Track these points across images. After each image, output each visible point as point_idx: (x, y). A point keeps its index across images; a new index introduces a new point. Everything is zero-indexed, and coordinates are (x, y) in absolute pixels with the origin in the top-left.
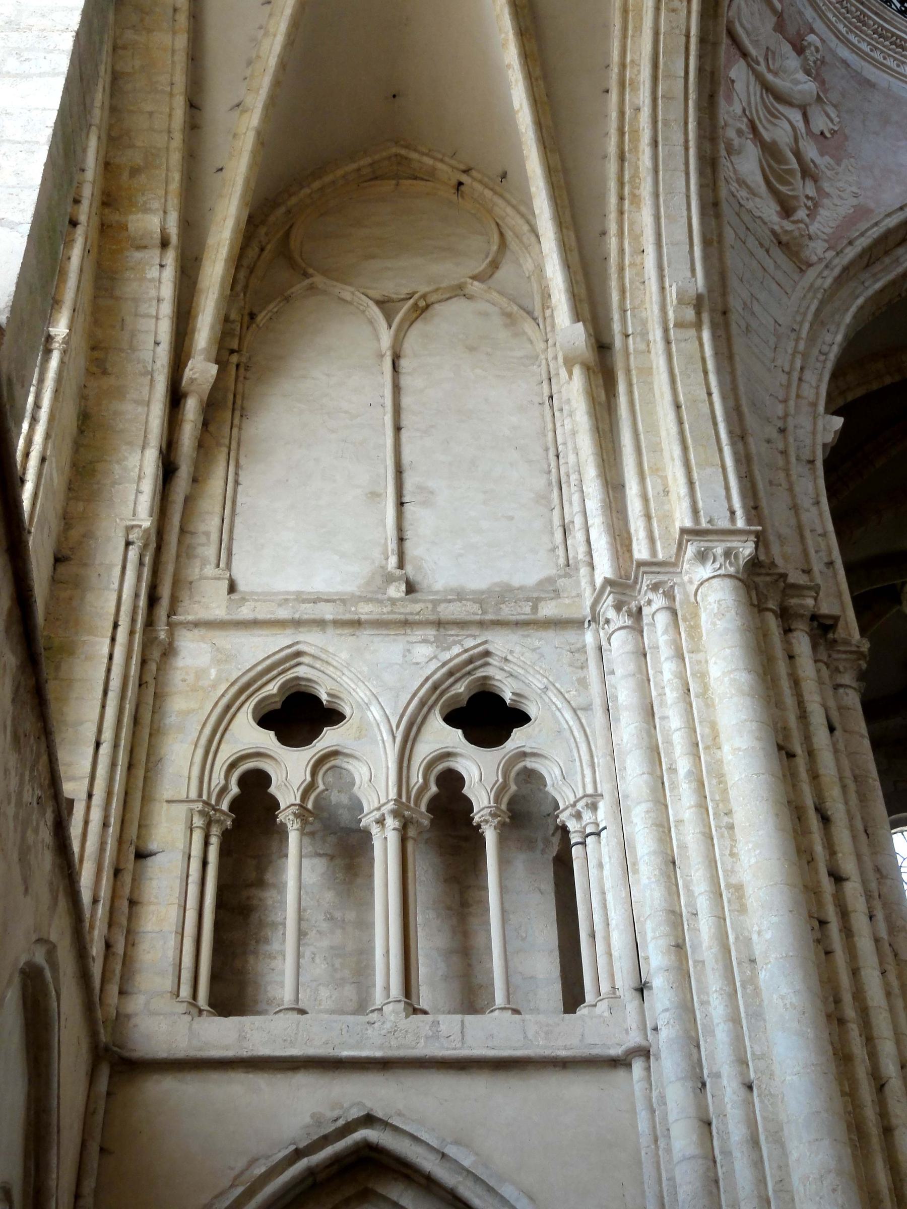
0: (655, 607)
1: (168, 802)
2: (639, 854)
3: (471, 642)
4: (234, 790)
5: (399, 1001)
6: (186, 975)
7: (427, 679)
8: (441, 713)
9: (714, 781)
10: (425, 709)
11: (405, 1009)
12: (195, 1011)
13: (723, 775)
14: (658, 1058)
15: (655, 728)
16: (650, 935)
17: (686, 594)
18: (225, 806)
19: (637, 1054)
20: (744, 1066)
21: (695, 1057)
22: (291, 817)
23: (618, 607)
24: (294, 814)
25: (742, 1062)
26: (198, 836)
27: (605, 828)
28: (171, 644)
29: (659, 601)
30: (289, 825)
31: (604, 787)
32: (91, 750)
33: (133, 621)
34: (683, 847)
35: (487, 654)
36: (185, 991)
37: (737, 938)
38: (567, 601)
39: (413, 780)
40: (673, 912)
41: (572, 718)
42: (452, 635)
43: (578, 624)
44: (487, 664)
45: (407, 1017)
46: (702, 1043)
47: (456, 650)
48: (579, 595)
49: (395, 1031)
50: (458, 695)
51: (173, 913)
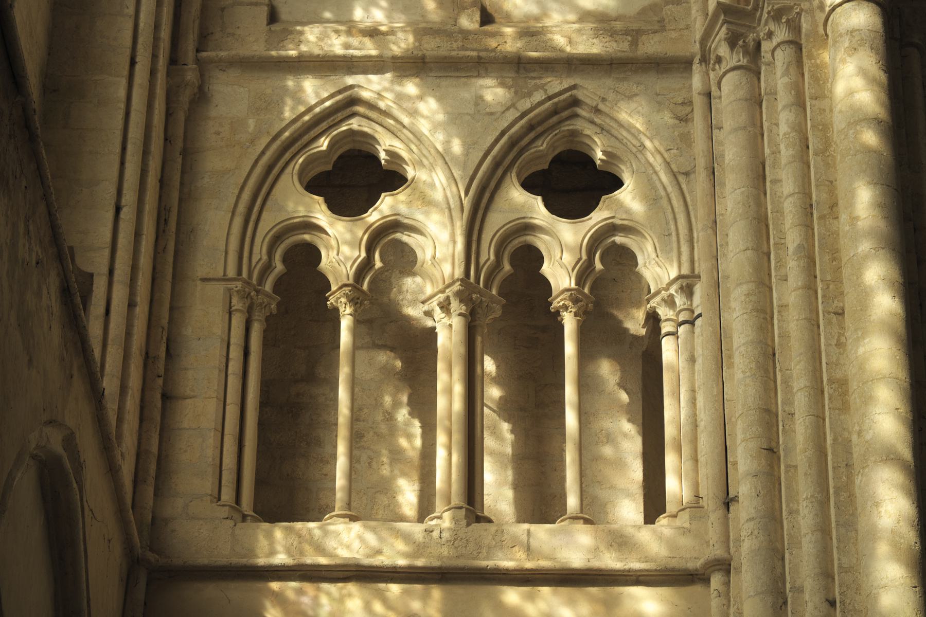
0: (775, 41)
1: (204, 280)
2: (735, 345)
3: (556, 84)
4: (279, 267)
5: (461, 508)
6: (228, 477)
7: (503, 133)
8: (518, 176)
9: (827, 258)
10: (500, 172)
11: (466, 517)
12: (237, 516)
13: (837, 251)
14: (738, 570)
15: (765, 194)
16: (740, 436)
17: (814, 23)
18: (268, 287)
19: (718, 567)
20: (830, 580)
21: (779, 570)
22: (343, 300)
23: (732, 42)
24: (346, 295)
25: (826, 575)
26: (238, 322)
27: (700, 315)
28: (201, 88)
29: (781, 34)
30: (341, 310)
31: (702, 267)
32: (110, 215)
33: (155, 57)
34: (785, 336)
35: (575, 102)
36: (227, 495)
37: (835, 440)
38: (674, 35)
39: (483, 259)
40: (768, 411)
41: (671, 183)
42: (534, 78)
43: (683, 65)
44: (576, 116)
45: (468, 525)
46: (787, 556)
47: (538, 97)
48: (688, 27)
49: (455, 540)
50: (539, 156)
51: (211, 408)
